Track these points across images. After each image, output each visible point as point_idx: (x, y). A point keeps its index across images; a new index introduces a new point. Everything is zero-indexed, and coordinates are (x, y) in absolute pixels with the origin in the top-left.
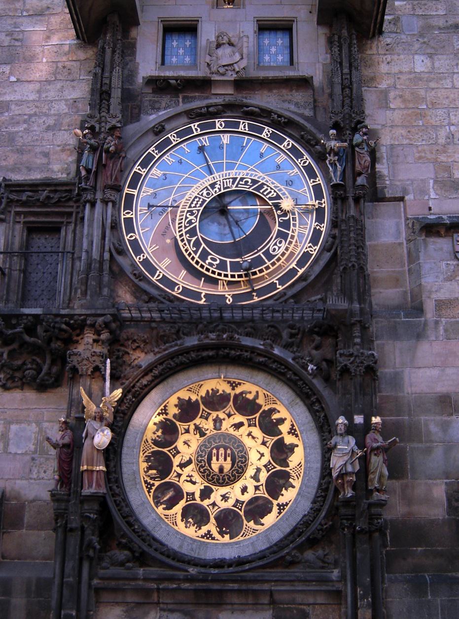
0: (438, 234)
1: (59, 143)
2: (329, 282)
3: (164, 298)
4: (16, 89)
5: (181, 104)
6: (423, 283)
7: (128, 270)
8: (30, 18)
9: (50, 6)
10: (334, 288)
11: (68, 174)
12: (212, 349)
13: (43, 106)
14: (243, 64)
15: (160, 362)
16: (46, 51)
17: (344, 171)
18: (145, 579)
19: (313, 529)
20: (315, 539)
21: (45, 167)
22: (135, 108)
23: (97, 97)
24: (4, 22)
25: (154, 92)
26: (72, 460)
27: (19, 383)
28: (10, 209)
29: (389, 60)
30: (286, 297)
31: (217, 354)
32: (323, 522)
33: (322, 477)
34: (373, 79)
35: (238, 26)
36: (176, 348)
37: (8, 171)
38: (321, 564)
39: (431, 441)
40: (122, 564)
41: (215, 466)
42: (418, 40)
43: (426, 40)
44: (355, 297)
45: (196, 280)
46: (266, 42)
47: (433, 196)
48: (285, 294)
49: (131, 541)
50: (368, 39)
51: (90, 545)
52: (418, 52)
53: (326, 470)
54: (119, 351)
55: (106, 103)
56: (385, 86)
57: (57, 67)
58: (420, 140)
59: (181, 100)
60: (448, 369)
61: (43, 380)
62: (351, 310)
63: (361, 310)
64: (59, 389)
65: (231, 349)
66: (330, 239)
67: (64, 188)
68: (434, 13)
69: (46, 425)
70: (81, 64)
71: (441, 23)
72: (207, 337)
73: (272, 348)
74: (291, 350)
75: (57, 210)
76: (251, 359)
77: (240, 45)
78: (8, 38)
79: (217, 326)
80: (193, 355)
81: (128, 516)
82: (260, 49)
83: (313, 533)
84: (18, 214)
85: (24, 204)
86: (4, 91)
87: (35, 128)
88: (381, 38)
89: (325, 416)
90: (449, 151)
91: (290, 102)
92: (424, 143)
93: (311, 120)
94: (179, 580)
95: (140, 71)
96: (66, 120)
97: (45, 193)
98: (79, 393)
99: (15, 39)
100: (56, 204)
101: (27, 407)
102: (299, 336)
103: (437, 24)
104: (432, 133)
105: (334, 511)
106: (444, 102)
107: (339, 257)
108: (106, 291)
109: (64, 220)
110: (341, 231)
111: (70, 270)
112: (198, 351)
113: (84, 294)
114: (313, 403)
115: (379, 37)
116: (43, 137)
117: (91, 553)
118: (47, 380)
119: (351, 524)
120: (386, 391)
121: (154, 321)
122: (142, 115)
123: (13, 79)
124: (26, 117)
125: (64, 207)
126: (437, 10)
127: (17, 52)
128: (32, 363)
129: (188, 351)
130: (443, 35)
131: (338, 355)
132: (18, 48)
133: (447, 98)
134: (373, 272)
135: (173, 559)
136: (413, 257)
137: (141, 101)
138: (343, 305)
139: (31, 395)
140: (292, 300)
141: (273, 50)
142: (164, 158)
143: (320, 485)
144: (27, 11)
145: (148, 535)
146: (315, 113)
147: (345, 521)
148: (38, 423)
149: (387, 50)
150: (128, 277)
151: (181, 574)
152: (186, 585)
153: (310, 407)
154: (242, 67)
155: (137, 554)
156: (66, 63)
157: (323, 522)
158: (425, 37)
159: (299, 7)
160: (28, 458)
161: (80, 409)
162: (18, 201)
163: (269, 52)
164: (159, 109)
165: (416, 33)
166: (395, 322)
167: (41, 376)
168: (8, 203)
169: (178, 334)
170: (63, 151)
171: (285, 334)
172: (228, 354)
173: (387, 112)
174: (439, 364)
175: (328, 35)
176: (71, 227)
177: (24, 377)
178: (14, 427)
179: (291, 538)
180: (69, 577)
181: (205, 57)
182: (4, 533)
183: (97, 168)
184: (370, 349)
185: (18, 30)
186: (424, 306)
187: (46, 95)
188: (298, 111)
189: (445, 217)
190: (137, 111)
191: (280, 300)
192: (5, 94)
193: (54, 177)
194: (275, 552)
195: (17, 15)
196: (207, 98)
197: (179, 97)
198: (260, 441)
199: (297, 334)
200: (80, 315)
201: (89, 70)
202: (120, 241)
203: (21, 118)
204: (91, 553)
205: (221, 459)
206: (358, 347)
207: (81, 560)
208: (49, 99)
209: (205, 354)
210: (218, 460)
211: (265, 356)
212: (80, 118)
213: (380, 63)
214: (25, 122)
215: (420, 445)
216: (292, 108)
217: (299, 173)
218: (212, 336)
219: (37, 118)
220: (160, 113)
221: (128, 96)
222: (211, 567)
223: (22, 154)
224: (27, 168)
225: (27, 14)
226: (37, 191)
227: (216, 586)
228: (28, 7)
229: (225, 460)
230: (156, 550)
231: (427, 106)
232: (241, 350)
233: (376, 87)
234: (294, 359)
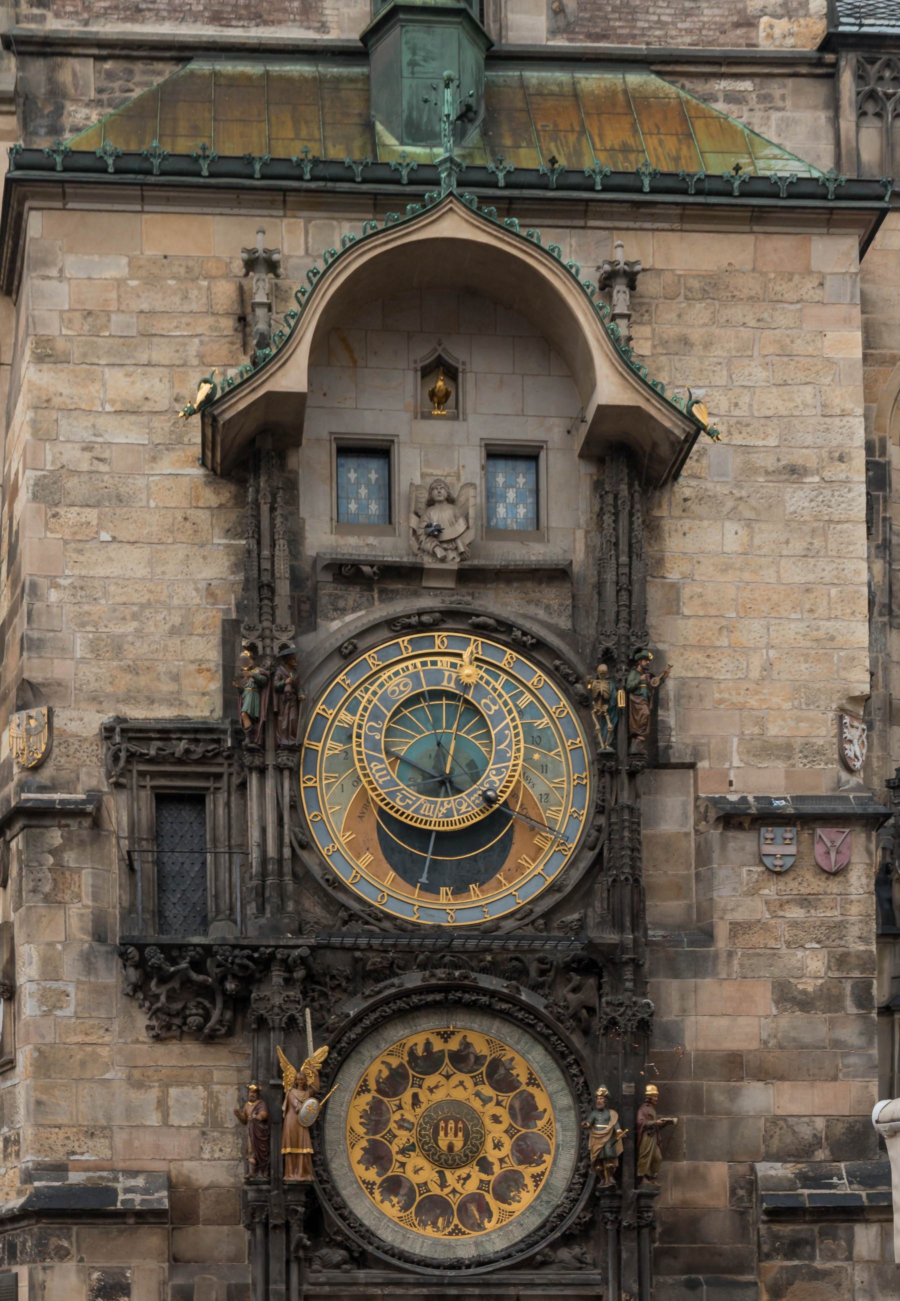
0: (740, 827)
1: (192, 658)
2: (589, 893)
3: (369, 915)
4: (112, 555)
5: (377, 603)
6: (715, 898)
7: (317, 871)
8: (119, 418)
9: (149, 396)
10: (597, 904)
11: (212, 711)
12: (440, 992)
13: (159, 589)
14: (470, 536)
15: (372, 1009)
16: (152, 485)
17: (616, 728)
18: (367, 1284)
19: (570, 1222)
20: (571, 1234)
21: (174, 700)
22: (305, 602)
23: (255, 595)
24: (75, 424)
25: (335, 580)
26: (269, 1140)
27: (178, 1033)
28: (130, 767)
29: (686, 529)
30: (533, 917)
31: (446, 998)
32: (582, 1215)
33: (580, 1159)
34: (660, 562)
35: (456, 456)
36: (393, 990)
37: (118, 702)
38: (579, 1265)
39: (714, 1113)
40: (337, 1266)
41: (443, 1143)
42: (731, 493)
43: (744, 493)
44: (628, 924)
45: (409, 887)
46: (500, 479)
47: (736, 762)
48: (532, 911)
49: (348, 1238)
50: (655, 488)
51: (300, 1245)
52: (731, 515)
53: (583, 1153)
54: (313, 991)
55: (266, 602)
56: (678, 576)
57: (174, 519)
58: (724, 670)
59: (376, 596)
60: (740, 1018)
61: (214, 1030)
62: (622, 942)
63: (635, 940)
64: (231, 1040)
65: (464, 992)
66: (594, 833)
67: (209, 737)
68: (761, 443)
69: (216, 1088)
70: (212, 516)
71: (770, 462)
72: (433, 975)
73: (518, 991)
74: (541, 992)
75: (200, 769)
76: (490, 1006)
77: (462, 499)
78: (87, 455)
79: (444, 956)
80: (415, 999)
81: (340, 1208)
82: (491, 495)
83: (569, 1228)
84: (142, 774)
85: (152, 761)
86: (94, 558)
87: (152, 629)
88: (676, 488)
89: (585, 1082)
90: (765, 691)
91: (538, 603)
92: (729, 676)
93: (571, 636)
94: (409, 1284)
95: (307, 535)
96: (200, 618)
97: (183, 745)
98: (268, 1051)
99: (97, 459)
100: (198, 762)
101: (189, 1064)
102: (552, 973)
103: (763, 464)
104: (741, 660)
105: (594, 1201)
106: (763, 608)
107: (605, 860)
108: (290, 906)
109: (209, 784)
110: (610, 825)
111: (227, 865)
112: (421, 994)
113: (261, 910)
114: (571, 1065)
115: (673, 486)
116: (166, 646)
117: (301, 1254)
118: (219, 1030)
119: (616, 1218)
120: (659, 1047)
121: (357, 948)
122: (319, 620)
123: (105, 536)
124: (135, 608)
125: (211, 764)
126: (766, 435)
127: (104, 484)
128: (197, 1007)
129: (408, 993)
130: (771, 484)
131: (604, 1005)
132: (106, 478)
133: (769, 600)
134: (648, 876)
135: (399, 1259)
136: (703, 857)
137: (315, 590)
138: (612, 937)
139: (193, 1048)
140: (541, 921)
141: (511, 495)
142: (356, 694)
143: (577, 1169)
144: (113, 402)
145: (367, 1231)
146: (573, 625)
147: (608, 1214)
148: (206, 1087)
149: (684, 511)
150: (319, 884)
151: (410, 1278)
152: (416, 1291)
153: (565, 1070)
154: (467, 542)
155: (356, 1255)
156: (189, 512)
157: (582, 1215)
158: (742, 488)
159: (551, 421)
160: (196, 1132)
161: (275, 1072)
162: (142, 755)
163: (504, 497)
164: (343, 611)
165: (729, 479)
166: (676, 953)
167: (210, 1024)
168: (128, 757)
169: (391, 970)
170: (200, 671)
171: (533, 969)
172: (460, 998)
173: (679, 621)
174: (730, 1011)
175: (595, 478)
176: (222, 798)
177: (185, 1023)
178: (173, 1092)
179: (541, 1233)
180: (275, 1282)
181: (408, 519)
182: (173, 1229)
183: (267, 715)
184: (644, 995)
185: (100, 440)
186: (715, 931)
187: (163, 569)
188: (550, 621)
189: (751, 799)
190: (306, 607)
191: (526, 921)
192: (96, 564)
193: (191, 713)
194: (522, 1251)
195: (95, 409)
196: (416, 594)
197: (373, 590)
198: (443, 1080)
199: (549, 970)
200: (267, 947)
201: (227, 526)
202: (301, 827)
203: (127, 611)
204: (301, 1254)
205: (451, 1134)
206: (630, 994)
207: (288, 1262)
208: (167, 577)
209: (430, 998)
210: (446, 1135)
211: (508, 1002)
212: (220, 615)
213: (673, 533)
214: (135, 617)
215: (699, 1117)
216: (541, 614)
217: (550, 725)
218: (440, 973)
219: (152, 610)
220: (348, 618)
221: (296, 581)
222: (446, 1268)
223: (137, 673)
224: (148, 698)
225: (112, 409)
226: (170, 739)
227: (453, 1291)
228: (111, 395)
229: (456, 1135)
230: (378, 1248)
231: (738, 613)
232: (478, 994)
233: (663, 577)
234: (546, 1007)
